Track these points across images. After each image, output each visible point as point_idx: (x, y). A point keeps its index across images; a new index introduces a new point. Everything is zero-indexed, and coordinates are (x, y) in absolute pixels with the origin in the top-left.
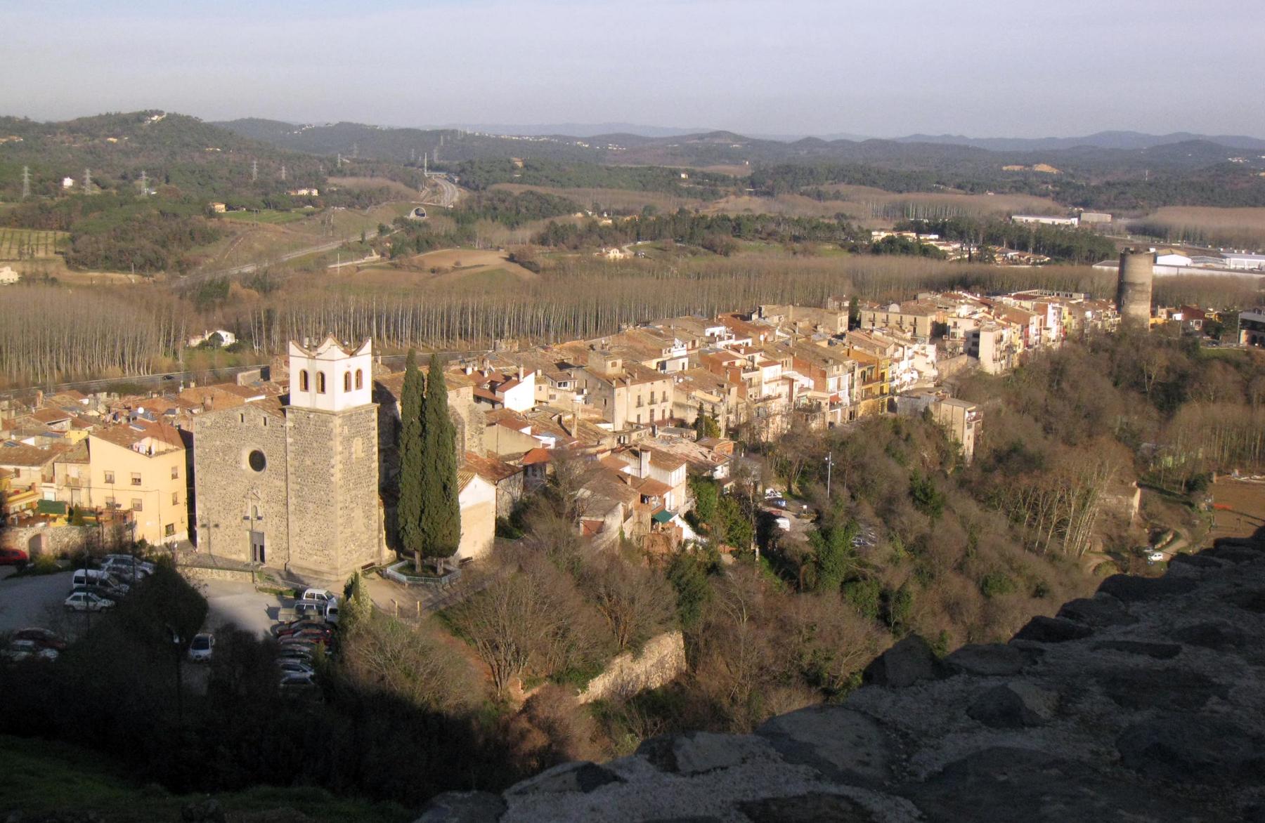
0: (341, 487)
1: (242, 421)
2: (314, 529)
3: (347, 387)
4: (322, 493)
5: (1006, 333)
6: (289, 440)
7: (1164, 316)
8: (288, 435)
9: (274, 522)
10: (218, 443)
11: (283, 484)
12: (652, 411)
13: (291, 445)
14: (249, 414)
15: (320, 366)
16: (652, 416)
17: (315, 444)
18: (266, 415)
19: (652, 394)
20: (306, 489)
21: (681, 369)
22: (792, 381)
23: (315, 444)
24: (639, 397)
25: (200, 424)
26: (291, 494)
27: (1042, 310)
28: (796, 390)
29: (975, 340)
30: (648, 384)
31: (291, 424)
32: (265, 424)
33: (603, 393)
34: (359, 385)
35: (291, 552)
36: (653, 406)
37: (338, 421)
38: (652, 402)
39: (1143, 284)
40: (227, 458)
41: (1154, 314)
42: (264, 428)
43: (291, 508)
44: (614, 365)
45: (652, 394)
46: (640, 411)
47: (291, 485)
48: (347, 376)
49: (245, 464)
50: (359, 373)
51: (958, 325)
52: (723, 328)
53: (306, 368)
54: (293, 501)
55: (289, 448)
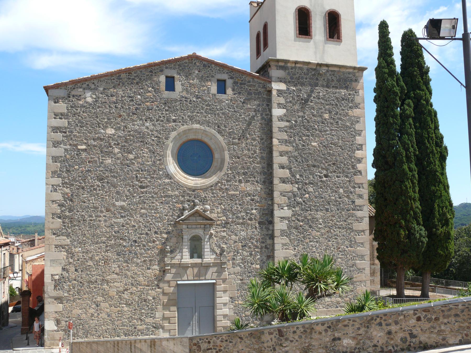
6: (277, 112)
8: (274, 105)
13: (281, 119)
18: (224, 76)
23: (326, 116)
43: (279, 226)
47: (279, 187)
55: (276, 124)
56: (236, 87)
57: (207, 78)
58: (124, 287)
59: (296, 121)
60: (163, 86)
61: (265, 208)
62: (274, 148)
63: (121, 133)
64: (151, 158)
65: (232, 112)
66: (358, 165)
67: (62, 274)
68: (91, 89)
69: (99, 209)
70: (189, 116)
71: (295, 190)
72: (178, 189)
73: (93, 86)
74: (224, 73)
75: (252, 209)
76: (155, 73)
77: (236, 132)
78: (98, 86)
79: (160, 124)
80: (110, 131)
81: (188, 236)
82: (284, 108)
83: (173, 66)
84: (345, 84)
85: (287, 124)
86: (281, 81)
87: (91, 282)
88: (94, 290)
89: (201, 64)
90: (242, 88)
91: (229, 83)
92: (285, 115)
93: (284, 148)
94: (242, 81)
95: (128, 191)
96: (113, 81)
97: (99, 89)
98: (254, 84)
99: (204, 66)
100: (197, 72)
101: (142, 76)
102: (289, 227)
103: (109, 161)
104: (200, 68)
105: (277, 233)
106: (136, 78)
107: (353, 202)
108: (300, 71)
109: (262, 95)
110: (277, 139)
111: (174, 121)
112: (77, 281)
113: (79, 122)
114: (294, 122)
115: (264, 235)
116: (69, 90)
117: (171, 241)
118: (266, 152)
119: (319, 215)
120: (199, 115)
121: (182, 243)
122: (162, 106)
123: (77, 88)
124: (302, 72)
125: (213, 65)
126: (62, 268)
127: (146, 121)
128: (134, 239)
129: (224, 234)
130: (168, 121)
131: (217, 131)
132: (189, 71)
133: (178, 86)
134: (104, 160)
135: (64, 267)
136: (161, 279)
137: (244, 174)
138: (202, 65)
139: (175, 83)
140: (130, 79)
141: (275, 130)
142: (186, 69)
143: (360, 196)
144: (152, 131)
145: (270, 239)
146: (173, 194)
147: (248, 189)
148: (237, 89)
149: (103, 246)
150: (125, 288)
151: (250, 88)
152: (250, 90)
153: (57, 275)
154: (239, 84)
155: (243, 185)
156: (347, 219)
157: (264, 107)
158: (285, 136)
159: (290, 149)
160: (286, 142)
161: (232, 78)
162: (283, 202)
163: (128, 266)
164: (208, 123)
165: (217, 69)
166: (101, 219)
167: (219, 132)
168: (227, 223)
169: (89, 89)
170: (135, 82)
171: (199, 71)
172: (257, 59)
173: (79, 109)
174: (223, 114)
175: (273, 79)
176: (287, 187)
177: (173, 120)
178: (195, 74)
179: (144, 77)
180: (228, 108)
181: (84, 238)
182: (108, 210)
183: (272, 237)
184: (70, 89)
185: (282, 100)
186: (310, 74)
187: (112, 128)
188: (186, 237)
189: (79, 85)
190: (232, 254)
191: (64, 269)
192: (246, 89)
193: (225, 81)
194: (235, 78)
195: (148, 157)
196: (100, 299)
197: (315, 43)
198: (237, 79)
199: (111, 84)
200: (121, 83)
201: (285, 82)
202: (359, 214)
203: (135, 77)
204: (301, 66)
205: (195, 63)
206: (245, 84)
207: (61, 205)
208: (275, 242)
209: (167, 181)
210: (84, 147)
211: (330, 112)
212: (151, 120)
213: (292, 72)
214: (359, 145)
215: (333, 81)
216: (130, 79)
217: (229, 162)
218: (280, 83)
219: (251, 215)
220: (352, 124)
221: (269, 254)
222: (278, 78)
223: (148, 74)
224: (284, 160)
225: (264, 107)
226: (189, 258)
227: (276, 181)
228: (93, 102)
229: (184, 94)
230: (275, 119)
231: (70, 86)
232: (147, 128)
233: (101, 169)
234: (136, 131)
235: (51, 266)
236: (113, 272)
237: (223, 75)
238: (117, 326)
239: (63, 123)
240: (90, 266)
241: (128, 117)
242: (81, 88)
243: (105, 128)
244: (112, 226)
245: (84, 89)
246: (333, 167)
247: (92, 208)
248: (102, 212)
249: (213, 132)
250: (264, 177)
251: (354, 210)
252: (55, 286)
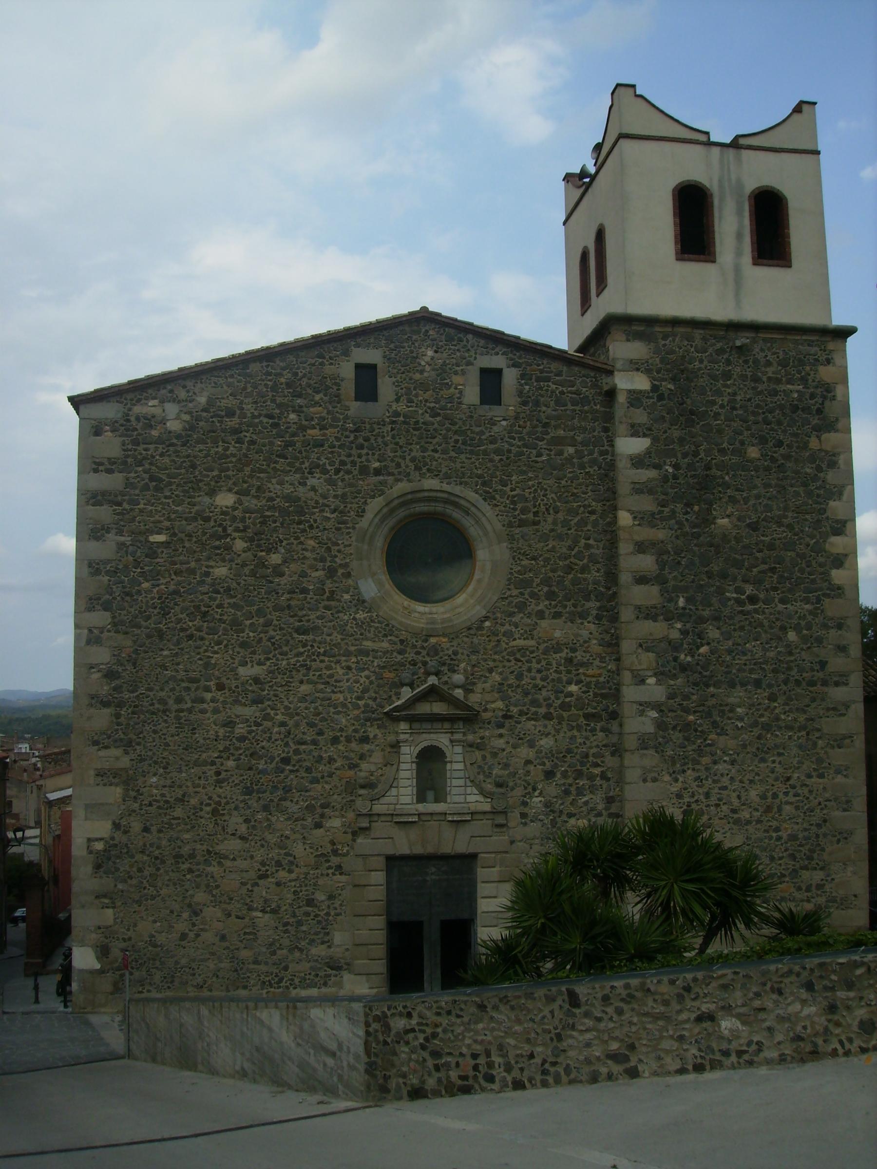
2: (753, 794)
4: (792, 636)
8: (622, 428)
9: (537, 801)
10: (225, 500)
13: (638, 462)
18: (496, 361)
20: (713, 633)
23: (753, 452)
31: (641, 383)
40: (275, 558)
42: (496, 411)
56: (527, 387)
57: (458, 368)
58: (259, 870)
59: (676, 467)
60: (349, 387)
61: (602, 679)
62: (622, 535)
63: (251, 503)
64: (323, 560)
65: (519, 447)
66: (834, 573)
67: (113, 838)
68: (179, 402)
69: (203, 683)
70: (413, 460)
71: (675, 635)
72: (385, 636)
73: (183, 394)
74: (497, 354)
75: (569, 683)
76: (331, 358)
77: (527, 495)
78: (195, 393)
79: (343, 480)
80: (225, 500)
81: (412, 748)
82: (645, 435)
83: (372, 340)
84: (799, 372)
85: (652, 474)
86: (638, 370)
87: (181, 856)
88: (188, 877)
89: (441, 334)
90: (541, 388)
91: (510, 378)
92: (648, 452)
94: (542, 371)
95: (269, 640)
96: (229, 380)
97: (198, 399)
98: (572, 378)
99: (450, 339)
100: (430, 353)
101: (298, 368)
102: (660, 725)
103: (221, 571)
104: (437, 345)
105: (631, 742)
106: (285, 372)
107: (823, 664)
108: (686, 343)
109: (592, 404)
110: (629, 511)
111: (377, 472)
112: (148, 856)
113: (152, 479)
114: (671, 470)
115: (597, 746)
116: (126, 404)
117: (371, 760)
118: (601, 545)
119: (737, 695)
120: (437, 455)
121: (399, 765)
122: (347, 437)
123: (147, 399)
124: (692, 346)
125: (470, 336)
126: (114, 823)
127: (310, 473)
128: (283, 755)
129: (500, 743)
130: (364, 471)
131: (481, 496)
132: (412, 352)
133: (386, 387)
134: (212, 567)
135: (117, 821)
136: (348, 851)
137: (551, 596)
138: (443, 337)
139: (379, 381)
140: (269, 374)
141: (624, 488)
142: (404, 347)
143: (842, 649)
144: (324, 497)
145: (613, 754)
146: (375, 646)
147: (558, 634)
148: (528, 392)
149: (211, 771)
150: (261, 872)
151: (561, 389)
152: (562, 393)
153: (101, 839)
154: (533, 380)
155: (544, 624)
156: (808, 706)
157: (596, 434)
158: (647, 504)
161: (514, 366)
162: (644, 667)
163: (268, 820)
165: (481, 344)
166: (205, 706)
167: (488, 497)
168: (505, 717)
169: (174, 401)
170: (283, 380)
171: (436, 352)
172: (583, 315)
173: (152, 446)
174: (497, 452)
175: (619, 365)
176: (657, 629)
177: (375, 469)
178: (427, 359)
179: (304, 368)
180: (509, 437)
181: (166, 754)
182: (221, 687)
183: (617, 751)
184: (129, 402)
185: (641, 417)
186: (710, 350)
187: (230, 490)
189: (150, 391)
190: (519, 792)
191: (116, 826)
192: (553, 392)
193: (499, 372)
194: (524, 366)
195: (315, 559)
196: (200, 897)
198: (528, 368)
199: (225, 388)
200: (249, 385)
201: (648, 372)
202: (838, 694)
203: (283, 369)
204: (689, 330)
205: (427, 331)
206: (548, 380)
207: (110, 675)
208: (626, 763)
209: (362, 616)
210: (161, 538)
211: (763, 441)
212: (325, 472)
213: (664, 345)
214: (837, 521)
215: (769, 364)
216: (269, 374)
217: (511, 569)
218: (635, 373)
219: (566, 697)
220: (819, 469)
221: (611, 794)
222: (631, 361)
223: (311, 361)
224: (647, 562)
225: (596, 434)
226: (415, 801)
227: (626, 614)
228: (185, 429)
229: (401, 407)
230: (622, 464)
231: (130, 396)
232: (314, 489)
233: (204, 589)
234: (288, 498)
235: (86, 819)
236: (233, 835)
237: (494, 357)
238: (243, 963)
240: (179, 818)
241: (268, 466)
242: (154, 398)
243: (212, 493)
244: (229, 724)
245: (162, 402)
246: (771, 577)
247: (182, 681)
248: (207, 689)
249: (472, 496)
250: (598, 604)
251: (825, 683)
252: (98, 867)
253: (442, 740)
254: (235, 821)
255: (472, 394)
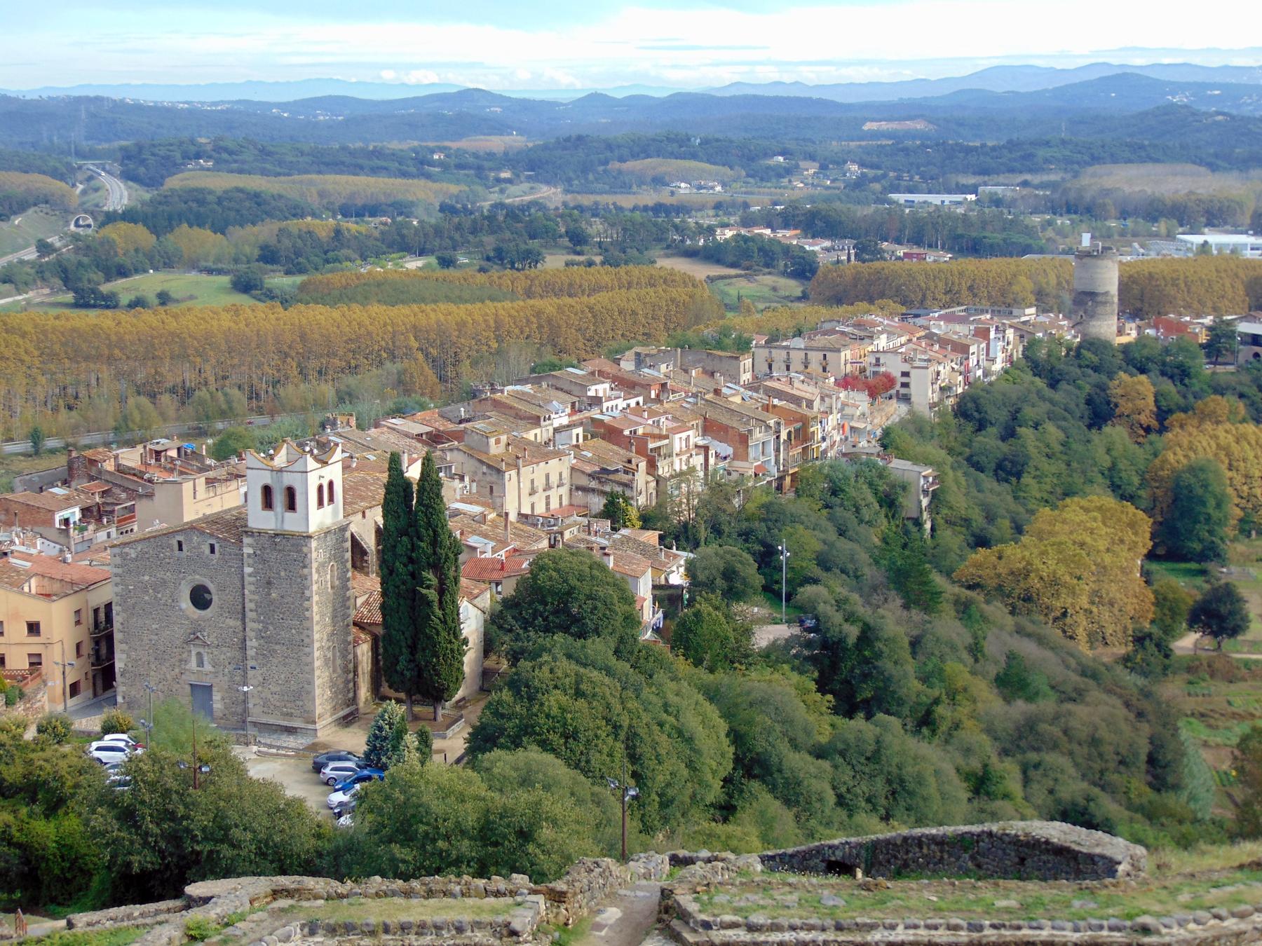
0: (318, 623)
1: (180, 549)
3: (320, 503)
5: (945, 370)
6: (248, 570)
7: (1134, 334)
10: (147, 578)
11: (239, 623)
12: (548, 497)
13: (250, 575)
14: (191, 540)
15: (288, 479)
16: (548, 504)
17: (283, 574)
18: (213, 541)
19: (547, 476)
20: (271, 628)
21: (574, 442)
22: (706, 449)
24: (532, 481)
25: (121, 555)
26: (250, 634)
27: (983, 334)
28: (712, 461)
29: (905, 380)
30: (542, 464)
31: (251, 551)
32: (213, 551)
33: (489, 478)
34: (331, 500)
35: (250, 705)
36: (547, 493)
37: (314, 544)
38: (548, 487)
39: (1106, 293)
41: (1120, 332)
43: (251, 653)
44: (498, 442)
45: (547, 476)
46: (535, 498)
47: (250, 625)
48: (320, 488)
49: (186, 604)
50: (331, 484)
51: (882, 361)
52: (607, 386)
53: (268, 481)
54: (252, 643)
55: (247, 579)
80: (147, 578)
93: (252, 597)
119: (277, 647)
133: (184, 547)
159: (256, 597)
160: (253, 593)
164: (205, 576)
176: (255, 625)
185: (251, 561)
188: (194, 653)
197: (276, 515)
239: (119, 571)
253: (201, 650)
254: (153, 667)
255: (207, 551)
